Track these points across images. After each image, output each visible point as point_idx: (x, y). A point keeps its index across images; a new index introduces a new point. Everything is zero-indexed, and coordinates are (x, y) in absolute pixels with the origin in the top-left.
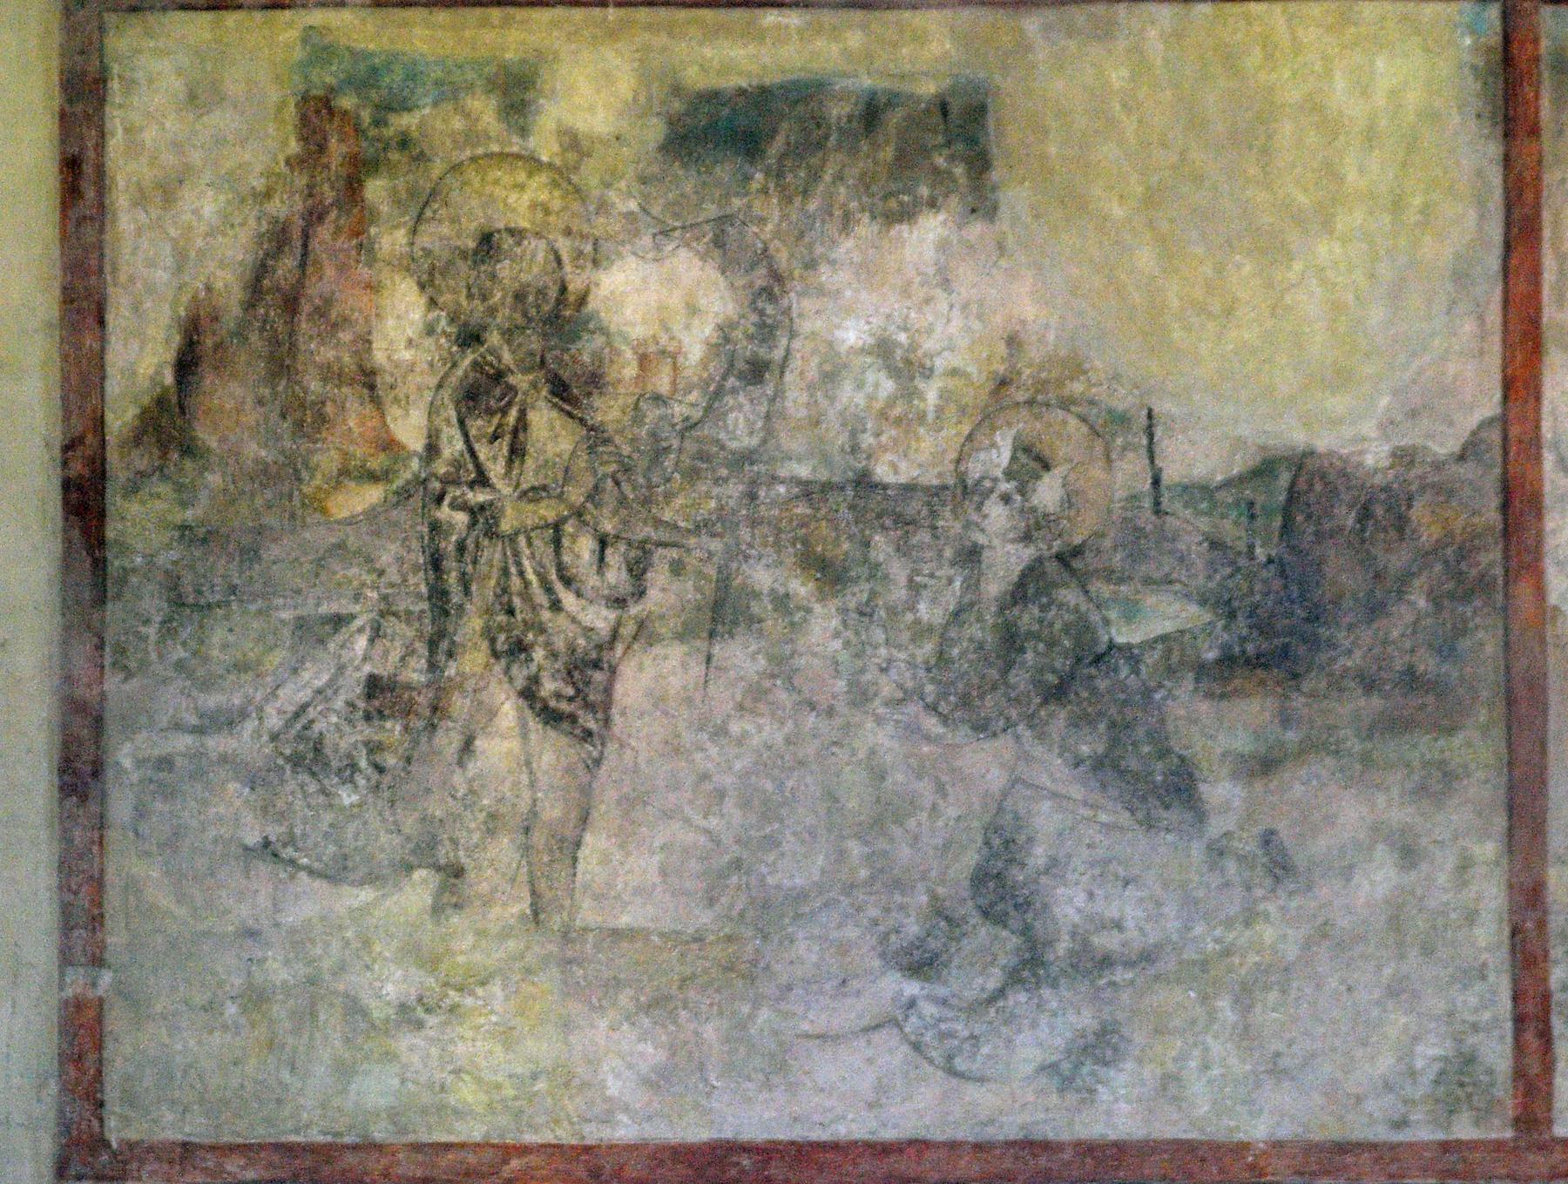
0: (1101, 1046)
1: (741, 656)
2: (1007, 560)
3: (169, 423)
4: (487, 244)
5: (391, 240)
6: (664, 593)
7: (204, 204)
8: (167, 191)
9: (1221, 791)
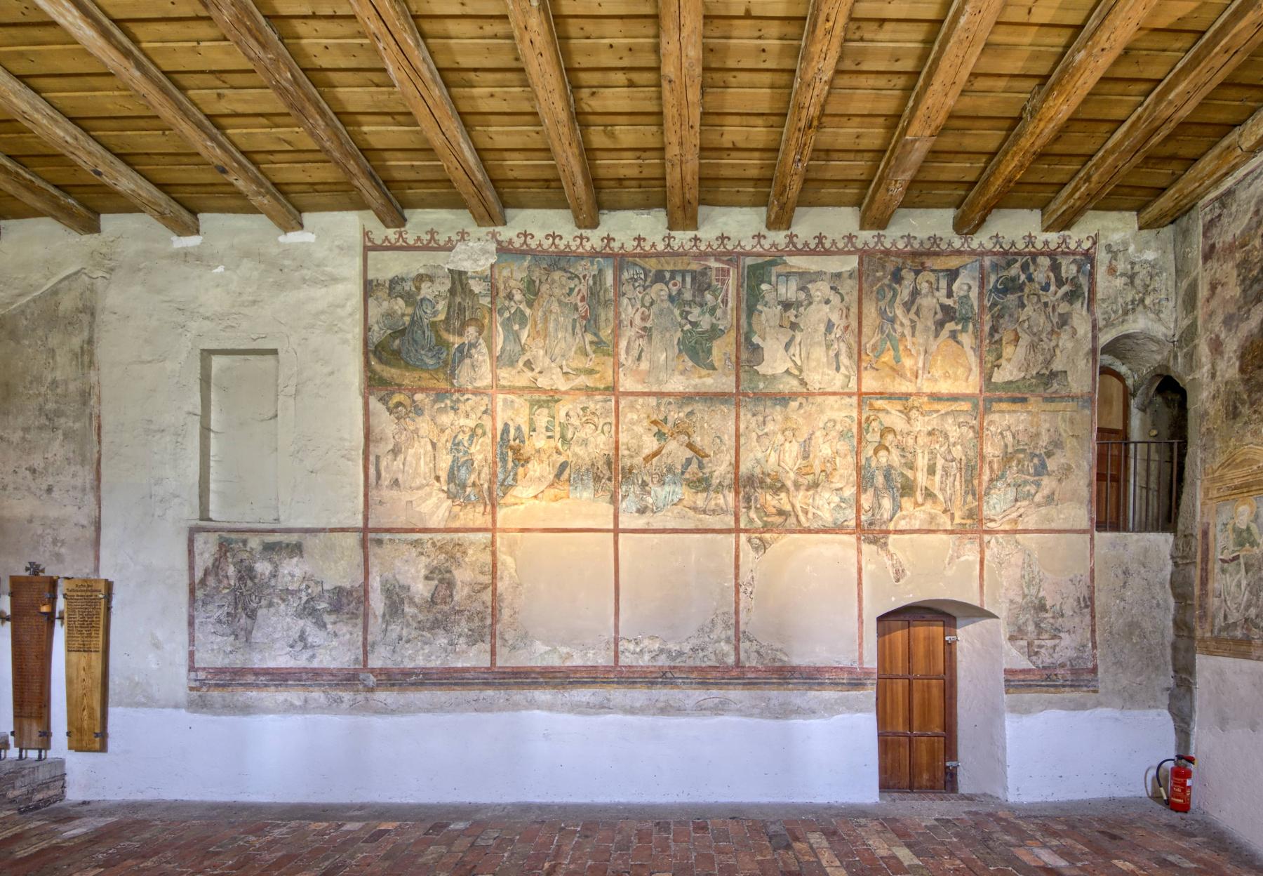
0: (313, 656)
1: (272, 610)
2: (305, 599)
3: (203, 582)
6: (263, 602)
7: (206, 555)
9: (329, 626)
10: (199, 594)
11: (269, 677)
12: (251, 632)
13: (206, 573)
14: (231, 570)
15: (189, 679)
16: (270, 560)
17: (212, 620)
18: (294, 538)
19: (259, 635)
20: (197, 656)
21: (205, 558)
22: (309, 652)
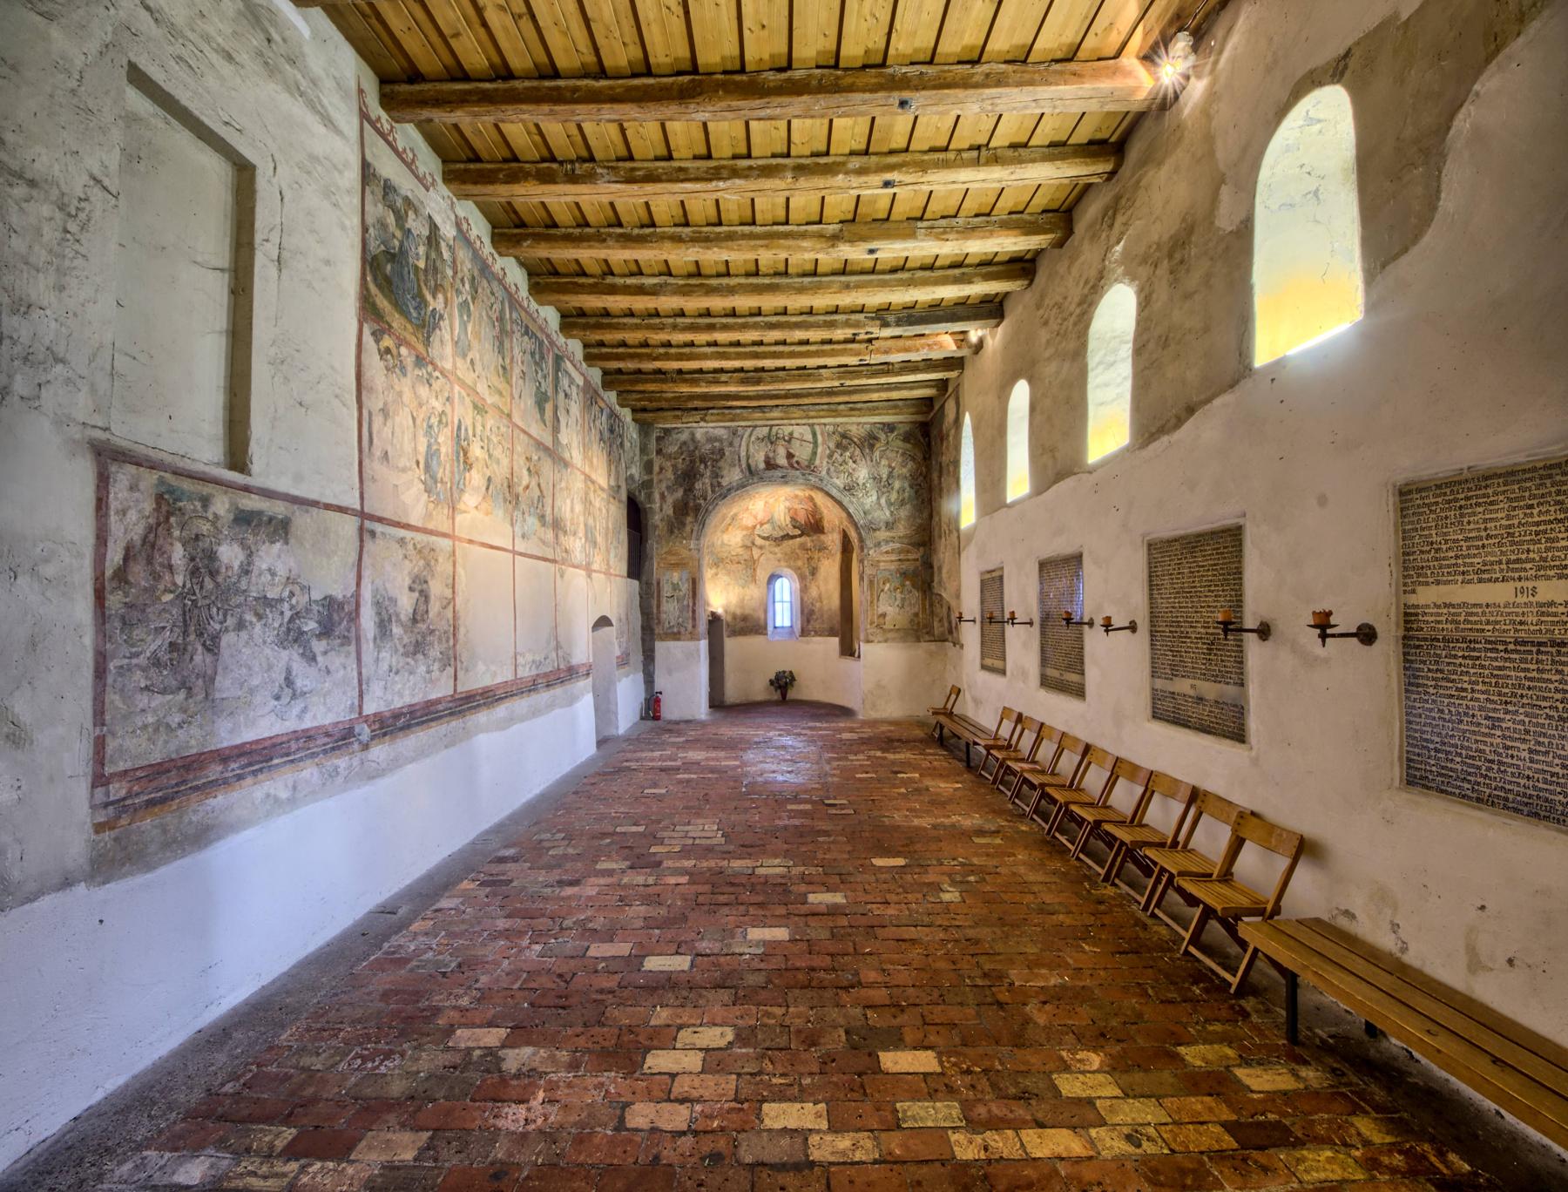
0: (305, 710)
1: (244, 635)
2: (288, 614)
3: (121, 575)
4: (197, 537)
5: (177, 533)
6: (230, 622)
8: (124, 512)
9: (320, 658)
10: (114, 601)
11: (244, 761)
12: (213, 680)
13: (128, 557)
14: (178, 554)
15: (93, 807)
16: (244, 545)
17: (142, 660)
18: (279, 509)
19: (228, 683)
20: (111, 745)
21: (128, 525)
22: (298, 706)
